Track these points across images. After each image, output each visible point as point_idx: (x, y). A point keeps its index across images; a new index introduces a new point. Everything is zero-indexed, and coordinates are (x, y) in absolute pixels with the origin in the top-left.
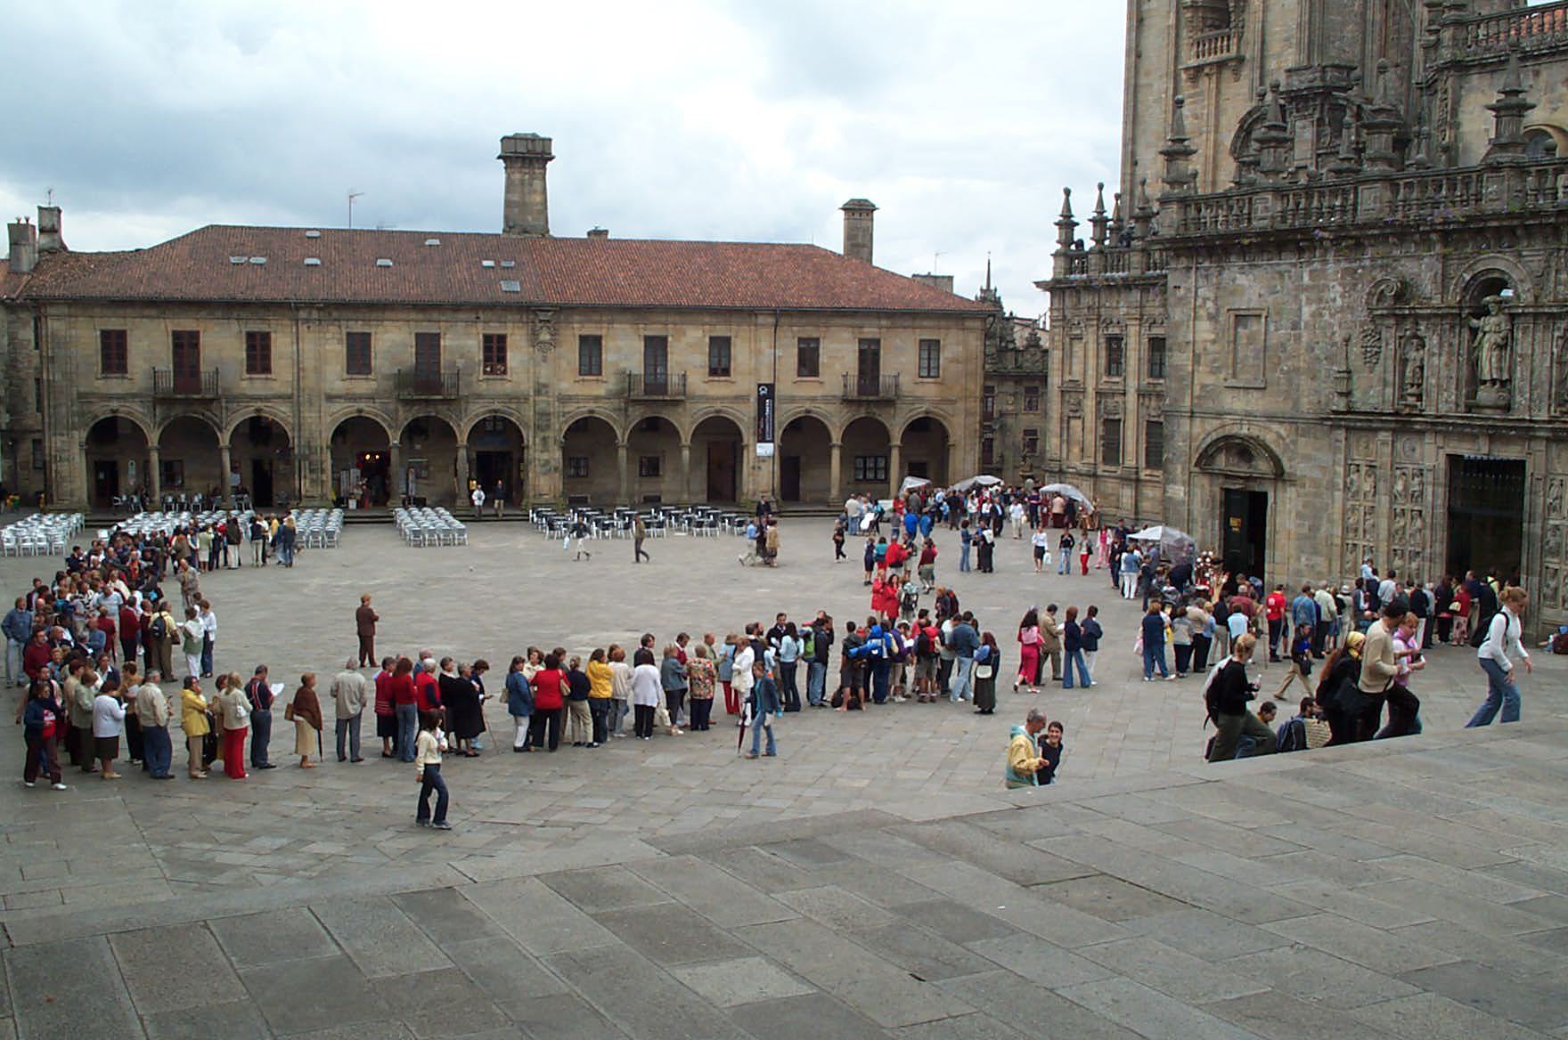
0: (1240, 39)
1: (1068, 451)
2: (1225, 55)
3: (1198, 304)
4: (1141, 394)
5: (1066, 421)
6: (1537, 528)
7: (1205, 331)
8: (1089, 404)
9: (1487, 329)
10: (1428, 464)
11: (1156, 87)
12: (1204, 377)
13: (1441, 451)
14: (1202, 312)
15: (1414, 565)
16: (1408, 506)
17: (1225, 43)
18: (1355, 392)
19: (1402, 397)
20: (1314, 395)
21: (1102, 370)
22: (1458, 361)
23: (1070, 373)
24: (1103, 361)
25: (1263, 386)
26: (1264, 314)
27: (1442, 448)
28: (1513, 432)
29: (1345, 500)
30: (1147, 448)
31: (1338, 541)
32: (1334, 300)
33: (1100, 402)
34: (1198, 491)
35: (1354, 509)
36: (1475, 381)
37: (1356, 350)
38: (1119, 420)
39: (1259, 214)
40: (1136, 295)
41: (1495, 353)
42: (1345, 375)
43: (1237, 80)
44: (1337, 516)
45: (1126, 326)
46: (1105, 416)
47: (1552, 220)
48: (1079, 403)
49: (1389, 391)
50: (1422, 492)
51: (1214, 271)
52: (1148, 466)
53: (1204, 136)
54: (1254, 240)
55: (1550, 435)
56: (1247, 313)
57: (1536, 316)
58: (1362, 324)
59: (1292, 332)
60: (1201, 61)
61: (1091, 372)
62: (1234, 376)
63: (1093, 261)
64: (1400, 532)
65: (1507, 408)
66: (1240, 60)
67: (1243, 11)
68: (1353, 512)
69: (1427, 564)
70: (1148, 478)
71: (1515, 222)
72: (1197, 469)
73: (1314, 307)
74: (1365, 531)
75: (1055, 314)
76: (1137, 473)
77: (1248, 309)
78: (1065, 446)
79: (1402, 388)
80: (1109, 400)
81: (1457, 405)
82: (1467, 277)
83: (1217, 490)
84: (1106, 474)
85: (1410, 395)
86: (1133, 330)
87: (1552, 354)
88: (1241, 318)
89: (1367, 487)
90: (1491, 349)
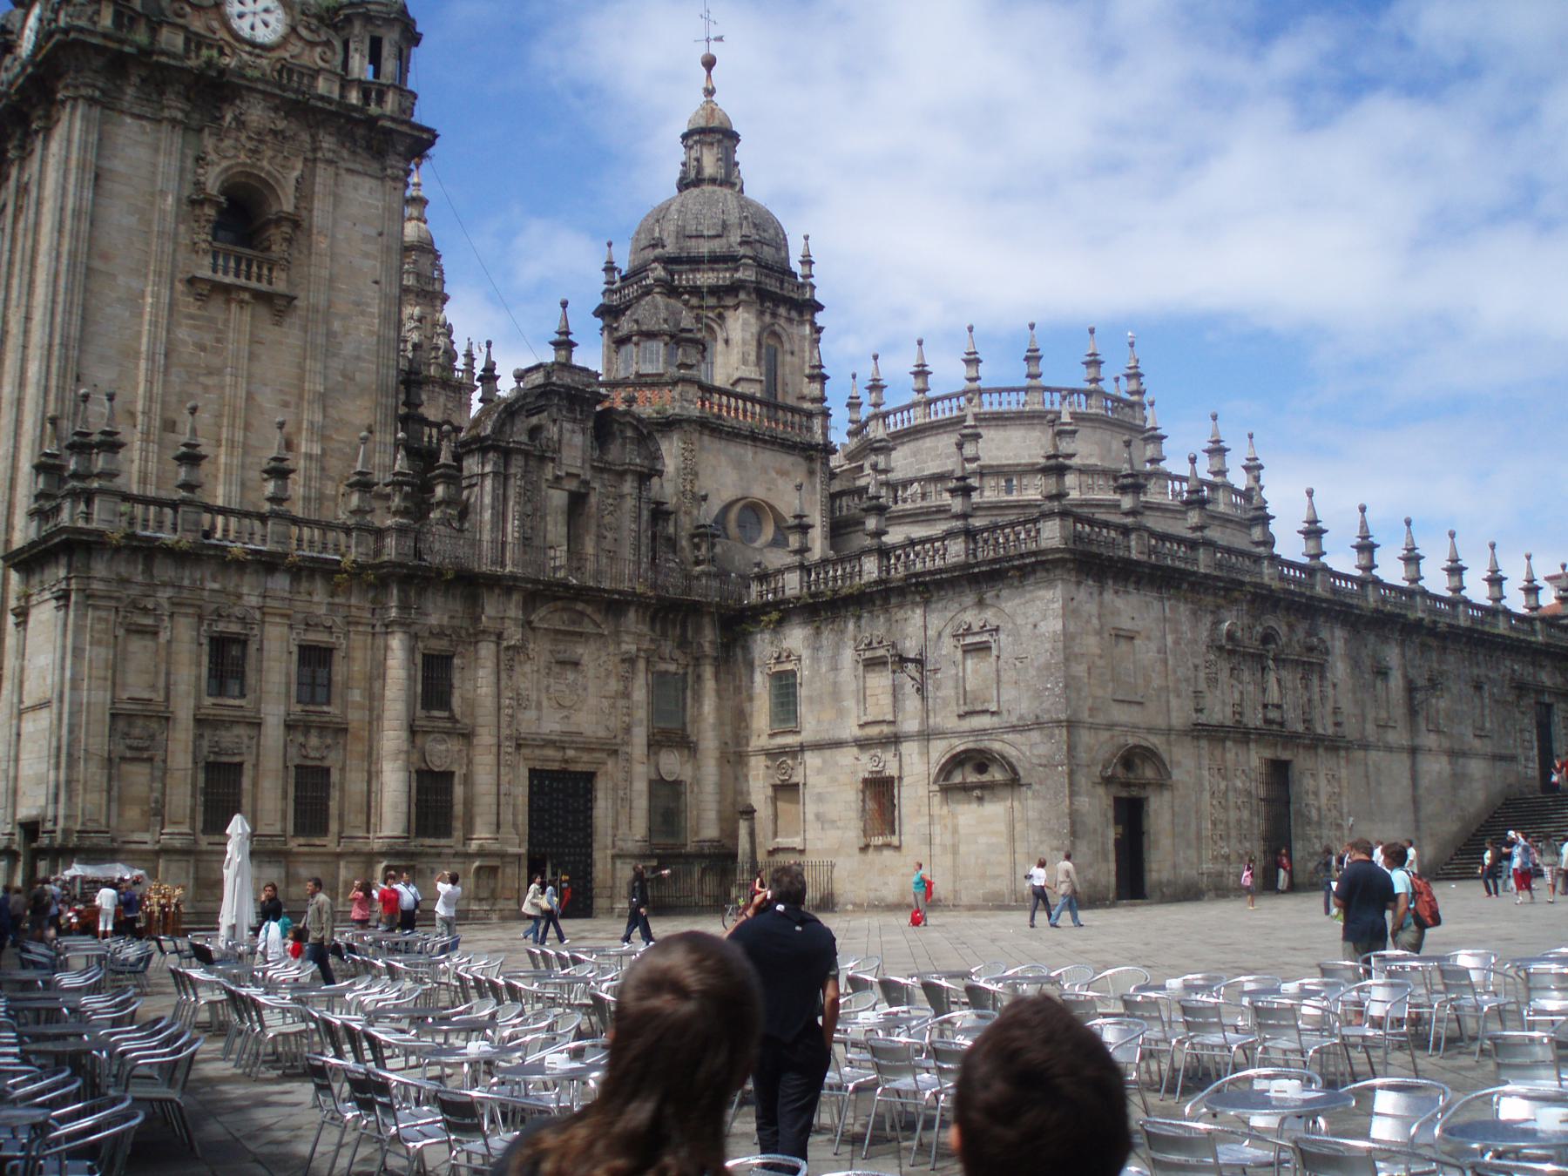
1: (120, 815)
2: (264, 286)
4: (290, 726)
11: (121, 280)
20: (1181, 714)
33: (201, 736)
37: (1202, 675)
38: (241, 764)
40: (280, 583)
46: (212, 758)
48: (152, 737)
51: (1095, 591)
52: (297, 833)
70: (306, 849)
78: (114, 806)
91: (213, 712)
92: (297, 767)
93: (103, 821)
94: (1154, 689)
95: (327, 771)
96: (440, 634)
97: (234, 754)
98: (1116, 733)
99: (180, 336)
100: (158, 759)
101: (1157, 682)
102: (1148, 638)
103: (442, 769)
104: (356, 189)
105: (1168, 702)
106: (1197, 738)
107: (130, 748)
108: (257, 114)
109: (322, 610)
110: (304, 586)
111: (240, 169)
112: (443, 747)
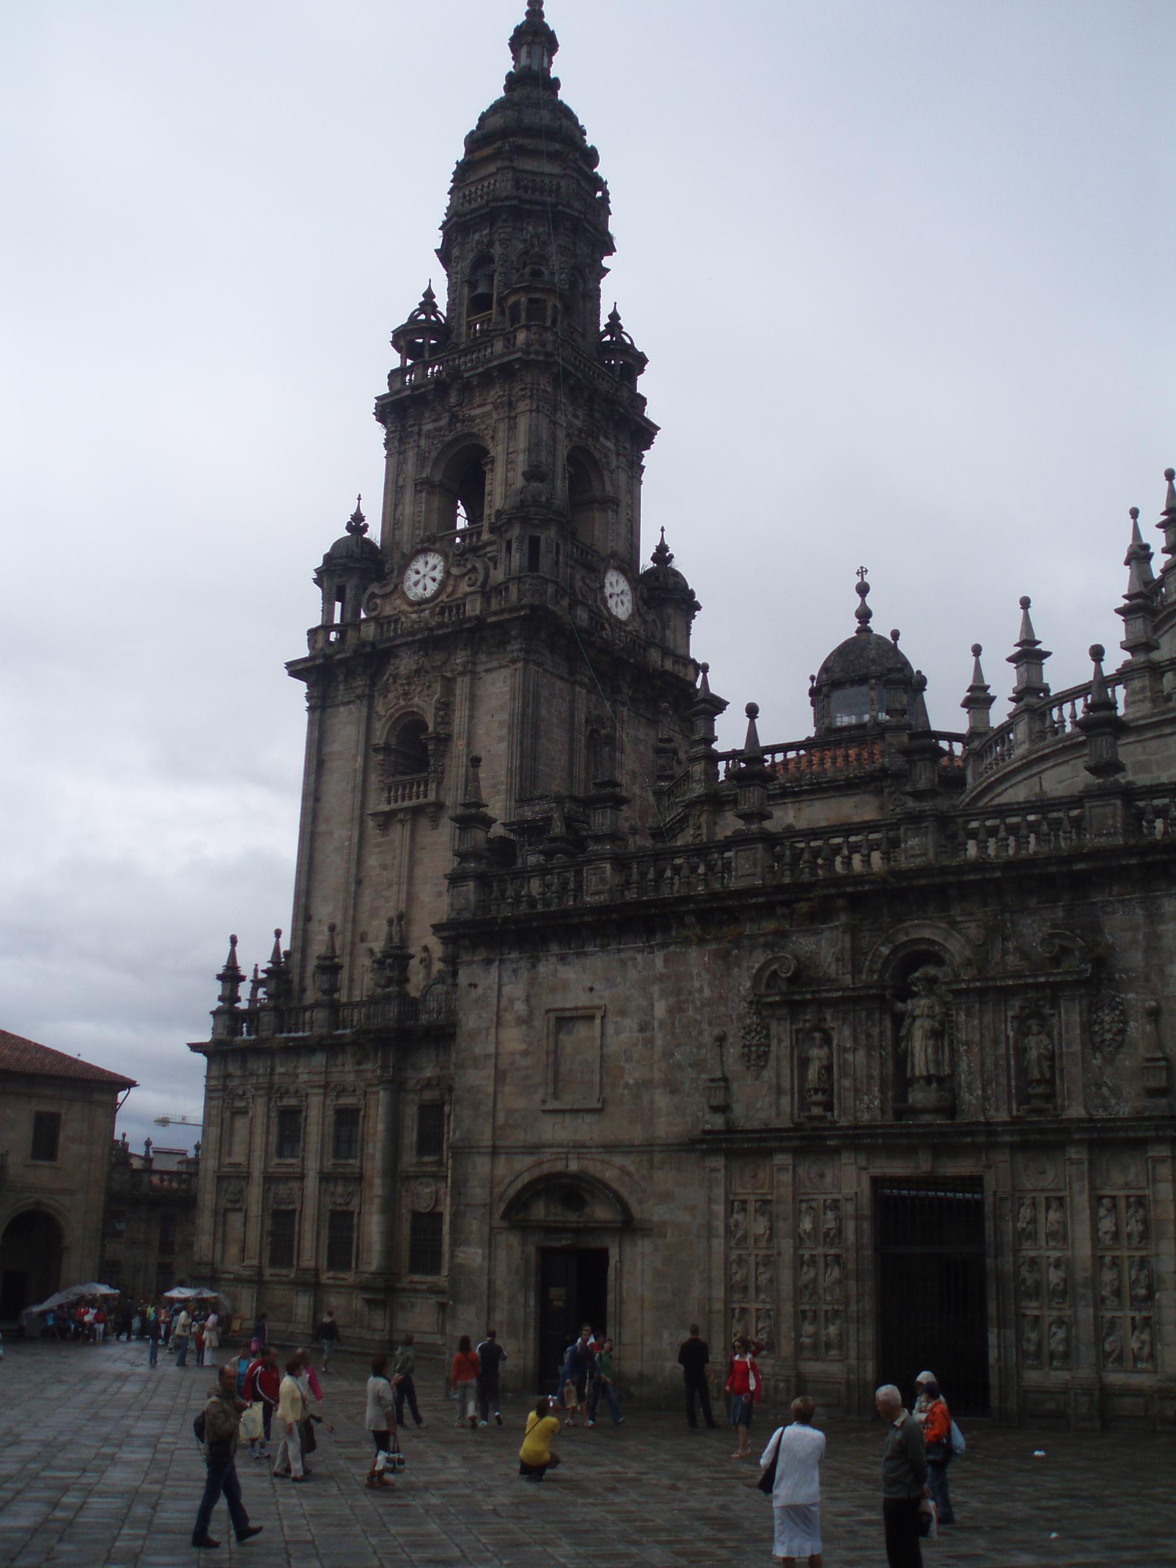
0: (439, 784)
2: (422, 800)
3: (502, 1006)
4: (324, 1177)
5: (221, 1216)
6: (1007, 1263)
7: (513, 1039)
8: (255, 1192)
9: (917, 1012)
10: (848, 1190)
12: (513, 1100)
13: (864, 1173)
14: (508, 1017)
15: (832, 1330)
16: (820, 1251)
17: (422, 789)
18: (734, 1106)
19: (804, 1106)
21: (273, 1148)
22: (881, 1056)
23: (230, 1155)
24: (274, 1139)
25: (599, 1105)
26: (599, 1014)
27: (865, 1169)
28: (969, 1140)
29: (728, 1248)
30: (329, 1245)
31: (719, 1306)
32: (701, 990)
33: (269, 1189)
34: (501, 1254)
35: (741, 1261)
36: (902, 1081)
37: (733, 1051)
38: (294, 1211)
39: (593, 889)
40: (319, 1060)
41: (931, 1042)
42: (723, 1084)
43: (435, 827)
44: (718, 1273)
45: (307, 1095)
46: (275, 1207)
47: (998, 874)
48: (241, 1192)
49: (786, 1101)
50: (840, 1230)
51: (524, 964)
52: (331, 1266)
53: (395, 888)
54: (588, 919)
55: (1017, 1138)
56: (574, 1013)
57: (982, 993)
58: (741, 1018)
59: (641, 1035)
60: (393, 806)
61: (258, 1154)
62: (556, 1096)
63: (266, 1019)
64: (811, 1286)
65: (951, 1111)
66: (439, 806)
67: (443, 756)
68: (739, 1265)
69: (853, 1328)
71: (951, 879)
72: (504, 1224)
73: (672, 1000)
74: (758, 1289)
75: (213, 1082)
76: (317, 1276)
77: (576, 1009)
78: (219, 1246)
79: (802, 1098)
80: (281, 1187)
81: (883, 1111)
82: (885, 951)
83: (531, 1249)
84: (274, 1279)
85: (816, 1104)
86: (315, 1101)
87: (1007, 1038)
88: (564, 1020)
89: (760, 1226)
90: (926, 1037)
91: (277, 1170)
92: (331, 1211)
93: (211, 1256)
94: (627, 1086)
95: (351, 1214)
96: (428, 1085)
97: (289, 1203)
98: (546, 1157)
99: (371, 863)
100: (244, 1208)
101: (632, 1075)
102: (623, 1013)
103: (428, 1210)
104: (493, 684)
105: (652, 1102)
106: (705, 1153)
107: (228, 1201)
108: (406, 663)
109: (351, 1078)
110: (339, 1061)
111: (400, 712)
112: (428, 1190)
